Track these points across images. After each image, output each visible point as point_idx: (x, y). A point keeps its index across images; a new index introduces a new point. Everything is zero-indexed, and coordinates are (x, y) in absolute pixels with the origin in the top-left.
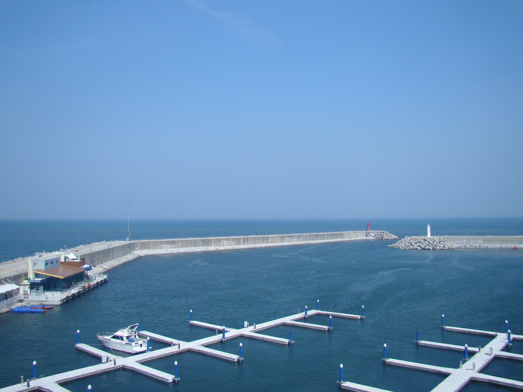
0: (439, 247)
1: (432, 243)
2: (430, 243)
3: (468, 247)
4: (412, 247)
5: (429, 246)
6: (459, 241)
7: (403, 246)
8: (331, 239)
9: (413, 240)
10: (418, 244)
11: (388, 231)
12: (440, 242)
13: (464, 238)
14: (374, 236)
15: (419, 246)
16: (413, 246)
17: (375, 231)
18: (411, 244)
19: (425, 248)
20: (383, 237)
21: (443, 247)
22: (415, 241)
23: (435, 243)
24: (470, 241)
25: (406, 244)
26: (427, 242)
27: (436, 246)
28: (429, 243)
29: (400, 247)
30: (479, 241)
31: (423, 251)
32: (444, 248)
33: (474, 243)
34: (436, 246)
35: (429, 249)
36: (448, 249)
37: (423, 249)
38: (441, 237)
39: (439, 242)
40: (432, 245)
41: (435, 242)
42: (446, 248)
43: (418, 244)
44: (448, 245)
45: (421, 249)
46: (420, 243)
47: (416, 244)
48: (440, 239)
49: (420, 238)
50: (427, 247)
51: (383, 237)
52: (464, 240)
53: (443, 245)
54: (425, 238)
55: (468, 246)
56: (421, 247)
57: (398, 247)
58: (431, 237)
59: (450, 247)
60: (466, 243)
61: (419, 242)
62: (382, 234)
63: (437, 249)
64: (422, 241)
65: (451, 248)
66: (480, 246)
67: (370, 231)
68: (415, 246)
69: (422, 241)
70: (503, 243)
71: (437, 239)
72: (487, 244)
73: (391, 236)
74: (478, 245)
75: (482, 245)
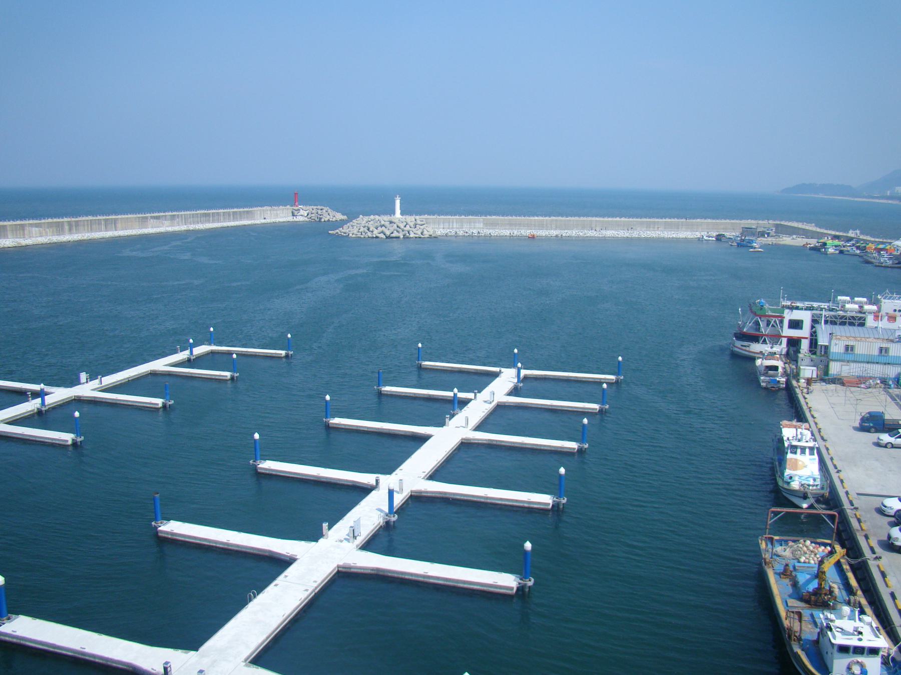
0: (415, 234)
1: (402, 227)
2: (400, 228)
3: (461, 234)
4: (370, 234)
5: (398, 232)
6: (447, 224)
7: (355, 232)
8: (231, 221)
9: (372, 222)
10: (380, 229)
11: (330, 208)
13: (455, 220)
14: (306, 215)
15: (382, 232)
16: (372, 232)
17: (308, 207)
18: (368, 229)
19: (392, 235)
20: (321, 217)
21: (420, 234)
22: (374, 223)
23: (408, 228)
24: (464, 224)
25: (359, 229)
26: (395, 226)
27: (409, 233)
28: (398, 227)
29: (351, 235)
30: (477, 225)
31: (388, 240)
32: (422, 236)
33: (470, 228)
34: (409, 233)
35: (398, 238)
36: (428, 238)
37: (388, 237)
38: (417, 217)
39: (414, 225)
40: (403, 231)
41: (408, 226)
43: (380, 229)
44: (428, 231)
45: (384, 237)
46: (383, 228)
47: (377, 229)
48: (416, 220)
49: (385, 219)
50: (395, 234)
51: (321, 217)
52: (455, 222)
54: (392, 218)
55: (461, 233)
56: (385, 235)
57: (347, 234)
58: (401, 217)
59: (431, 233)
60: (457, 228)
61: (382, 226)
62: (320, 212)
63: (410, 238)
64: (387, 224)
65: (433, 235)
66: (479, 233)
67: (300, 206)
68: (376, 232)
69: (387, 224)
70: (514, 227)
71: (411, 220)
72: (490, 229)
73: (336, 216)
74: (475, 231)
75: (482, 232)
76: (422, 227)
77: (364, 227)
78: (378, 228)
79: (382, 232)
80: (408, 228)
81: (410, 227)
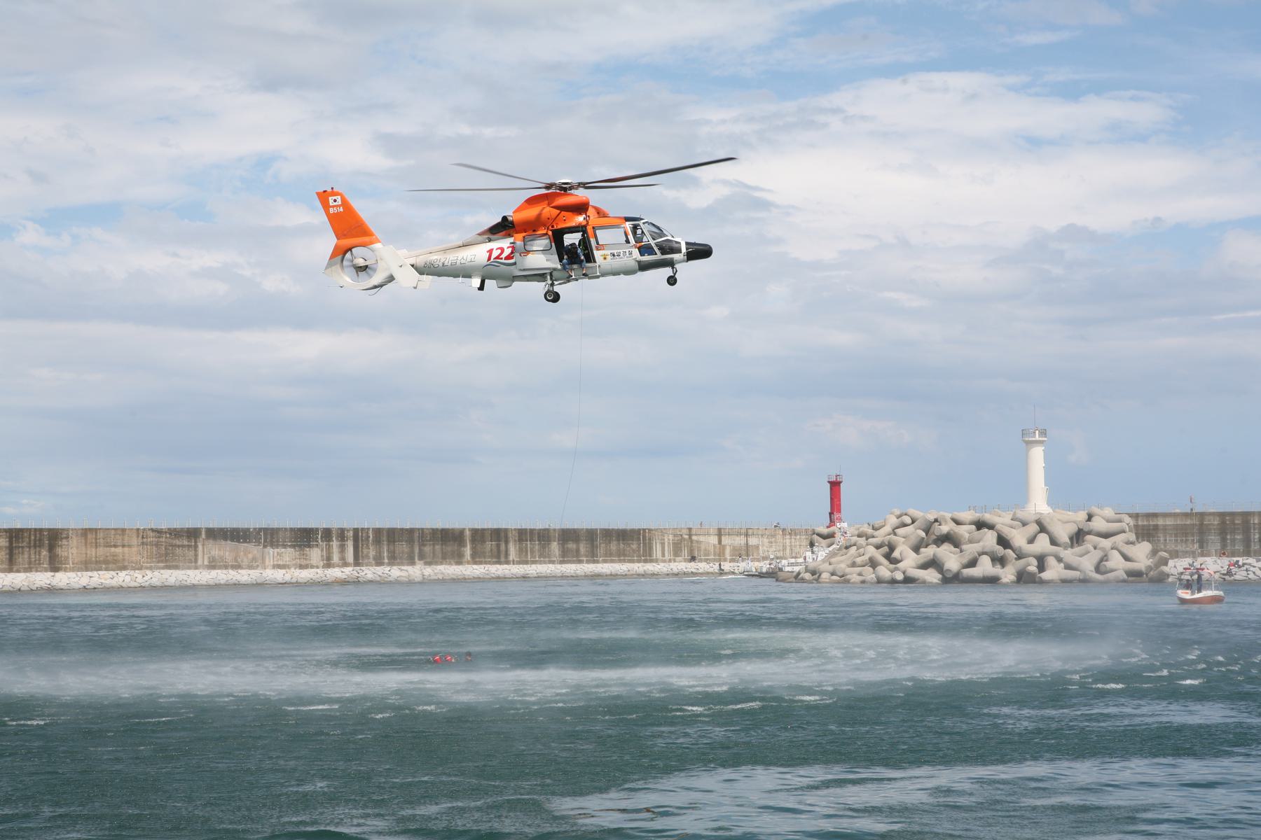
4: (884, 571)
5: (1000, 561)
10: (929, 552)
12: (1078, 537)
15: (933, 563)
26: (989, 539)
35: (993, 581)
36: (1124, 581)
42: (1111, 576)
44: (1126, 558)
46: (946, 549)
47: (916, 549)
48: (1090, 517)
50: (985, 567)
53: (1097, 555)
61: (947, 538)
64: (964, 531)
68: (910, 562)
76: (1106, 543)
77: (878, 547)
78: (922, 550)
79: (933, 563)
80: (1043, 544)
81: (1053, 542)
